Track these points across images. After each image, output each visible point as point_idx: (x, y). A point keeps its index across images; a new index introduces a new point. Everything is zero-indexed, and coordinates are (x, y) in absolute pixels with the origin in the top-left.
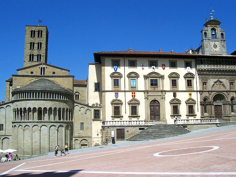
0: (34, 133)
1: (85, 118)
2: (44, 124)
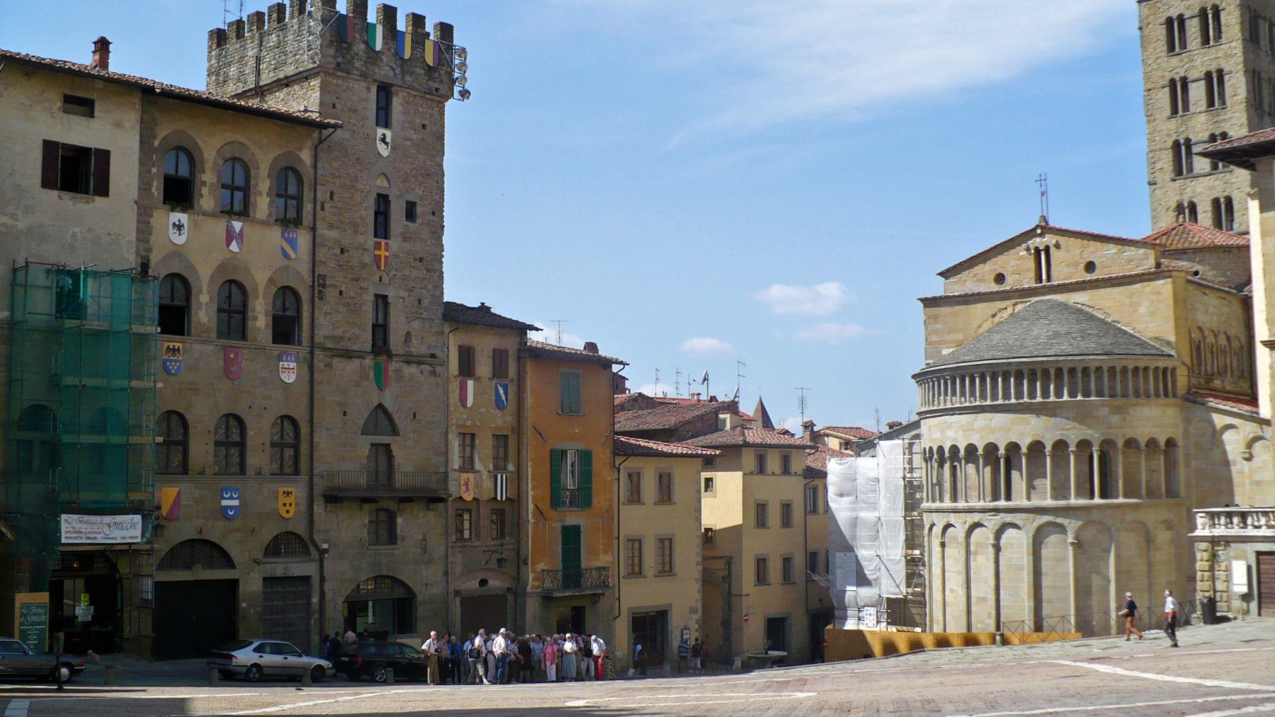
0: (975, 561)
1: (1247, 486)
2: (1009, 518)
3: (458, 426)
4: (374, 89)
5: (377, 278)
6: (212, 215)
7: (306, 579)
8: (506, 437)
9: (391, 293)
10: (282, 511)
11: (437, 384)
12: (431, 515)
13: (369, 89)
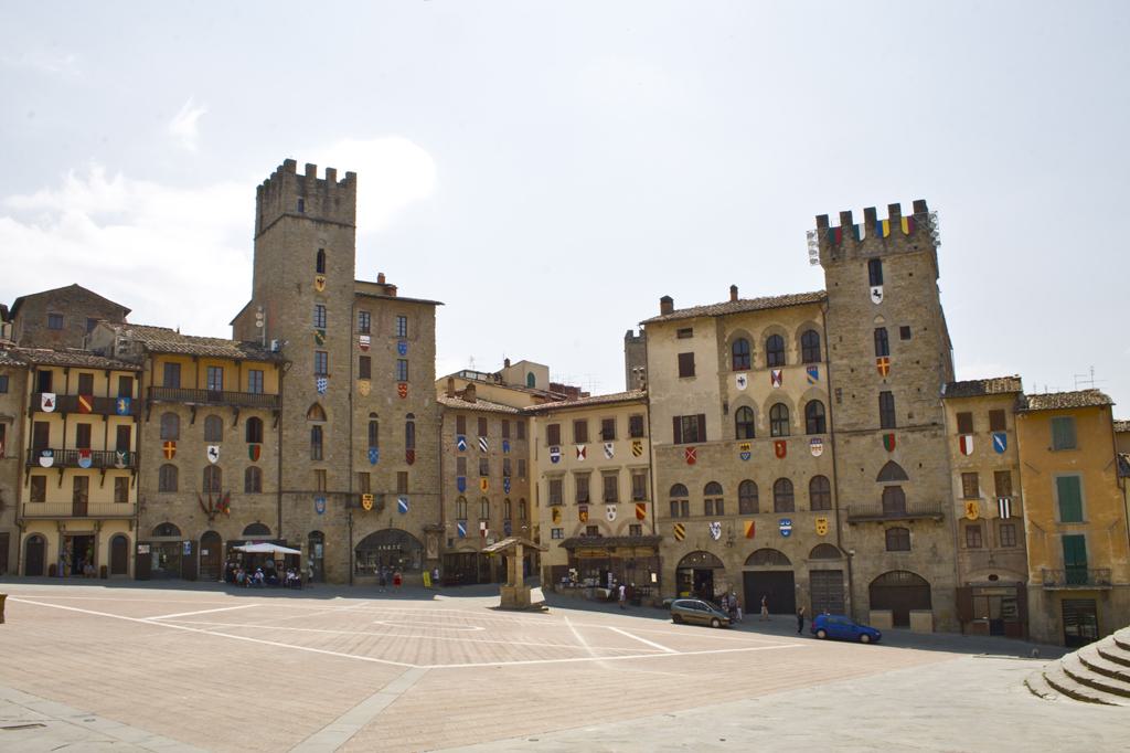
3: (960, 468)
4: (866, 265)
5: (882, 381)
6: (762, 369)
7: (841, 571)
8: (1009, 472)
9: (894, 389)
10: (819, 531)
11: (939, 442)
12: (940, 531)
13: (862, 265)
